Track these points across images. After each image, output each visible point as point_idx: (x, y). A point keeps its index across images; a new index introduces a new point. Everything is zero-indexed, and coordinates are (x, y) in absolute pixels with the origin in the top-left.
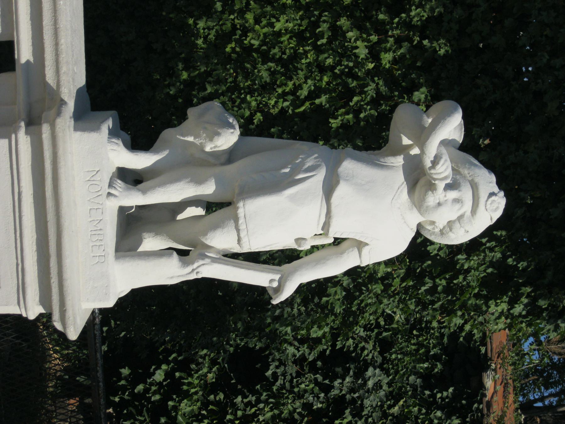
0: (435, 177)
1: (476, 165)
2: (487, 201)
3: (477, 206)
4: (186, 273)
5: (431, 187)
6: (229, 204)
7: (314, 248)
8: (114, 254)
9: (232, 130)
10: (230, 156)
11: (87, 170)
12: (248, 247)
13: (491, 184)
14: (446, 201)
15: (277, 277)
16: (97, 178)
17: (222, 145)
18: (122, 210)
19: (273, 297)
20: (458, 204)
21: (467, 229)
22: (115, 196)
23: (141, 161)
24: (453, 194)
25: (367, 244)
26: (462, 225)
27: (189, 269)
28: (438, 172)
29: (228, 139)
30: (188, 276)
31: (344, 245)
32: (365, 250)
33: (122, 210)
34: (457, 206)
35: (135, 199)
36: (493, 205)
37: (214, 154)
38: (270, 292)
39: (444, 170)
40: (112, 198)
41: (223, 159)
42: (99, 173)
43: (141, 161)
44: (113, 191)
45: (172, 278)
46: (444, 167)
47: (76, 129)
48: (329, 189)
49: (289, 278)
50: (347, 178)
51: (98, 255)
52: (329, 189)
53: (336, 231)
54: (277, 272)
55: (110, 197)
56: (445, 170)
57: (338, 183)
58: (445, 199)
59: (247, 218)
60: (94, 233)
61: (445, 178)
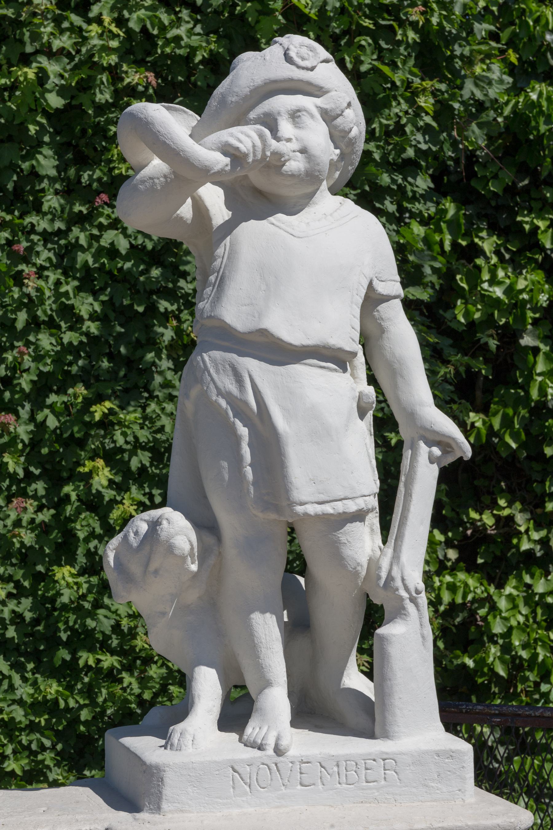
0: (259, 156)
1: (232, 81)
2: (299, 67)
3: (309, 83)
4: (416, 611)
5: (274, 164)
6: (292, 531)
7: (372, 380)
8: (379, 740)
9: (165, 522)
10: (206, 525)
11: (232, 790)
12: (372, 497)
13: (268, 58)
14: (297, 139)
15: (423, 449)
16: (245, 770)
17: (192, 545)
18: (296, 723)
19: (458, 455)
20: (303, 118)
21: (345, 105)
22: (278, 739)
23: (208, 687)
24: (286, 127)
25: (370, 285)
26: (339, 113)
27: (410, 607)
28: (251, 150)
29: (177, 527)
30: (421, 608)
31: (371, 329)
32: (382, 288)
33: (296, 723)
34: (306, 118)
35: (276, 701)
36: (306, 56)
37: (204, 554)
38: (450, 459)
39: (246, 137)
40: (284, 743)
41: (210, 540)
42: (236, 768)
43: (208, 687)
44: (271, 742)
45: (423, 637)
46: (242, 137)
47: (158, 809)
48: (280, 353)
49: (429, 427)
50: (257, 315)
51: (383, 771)
52: (280, 353)
53: (347, 338)
54: (414, 448)
55: (282, 748)
56: (248, 136)
57: (264, 332)
58: (294, 140)
59: (323, 498)
60: (343, 779)
61: (261, 136)
